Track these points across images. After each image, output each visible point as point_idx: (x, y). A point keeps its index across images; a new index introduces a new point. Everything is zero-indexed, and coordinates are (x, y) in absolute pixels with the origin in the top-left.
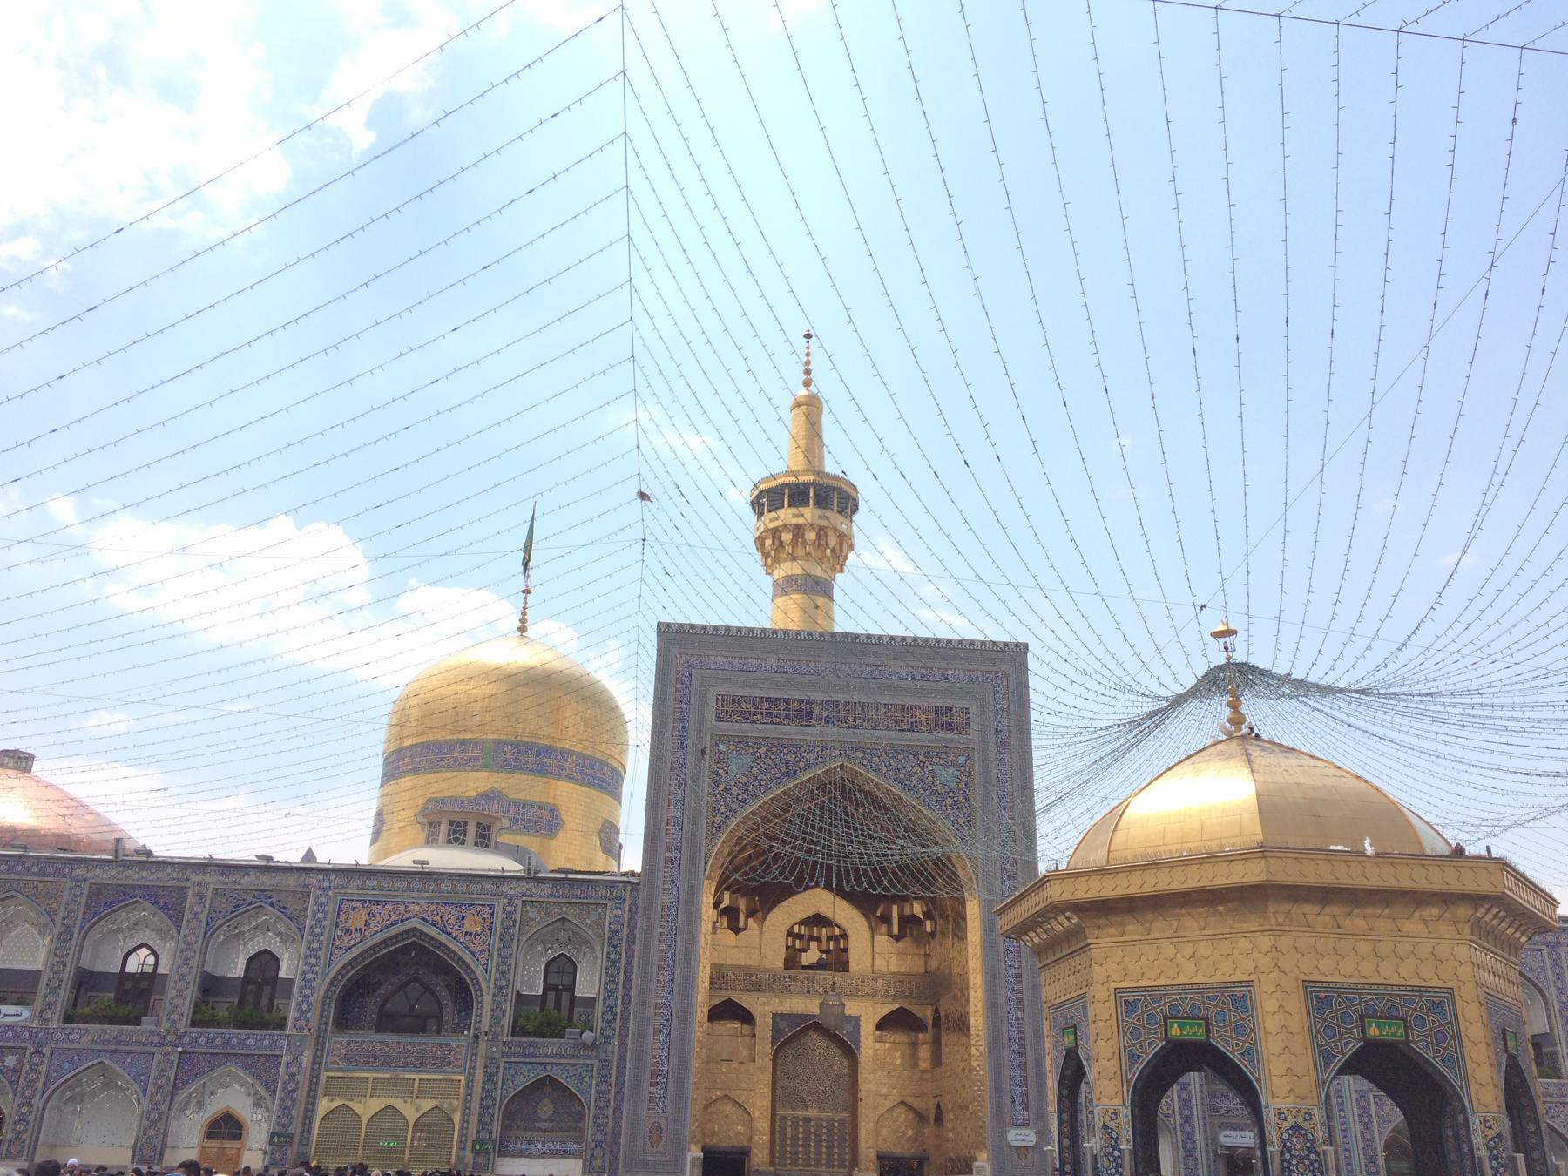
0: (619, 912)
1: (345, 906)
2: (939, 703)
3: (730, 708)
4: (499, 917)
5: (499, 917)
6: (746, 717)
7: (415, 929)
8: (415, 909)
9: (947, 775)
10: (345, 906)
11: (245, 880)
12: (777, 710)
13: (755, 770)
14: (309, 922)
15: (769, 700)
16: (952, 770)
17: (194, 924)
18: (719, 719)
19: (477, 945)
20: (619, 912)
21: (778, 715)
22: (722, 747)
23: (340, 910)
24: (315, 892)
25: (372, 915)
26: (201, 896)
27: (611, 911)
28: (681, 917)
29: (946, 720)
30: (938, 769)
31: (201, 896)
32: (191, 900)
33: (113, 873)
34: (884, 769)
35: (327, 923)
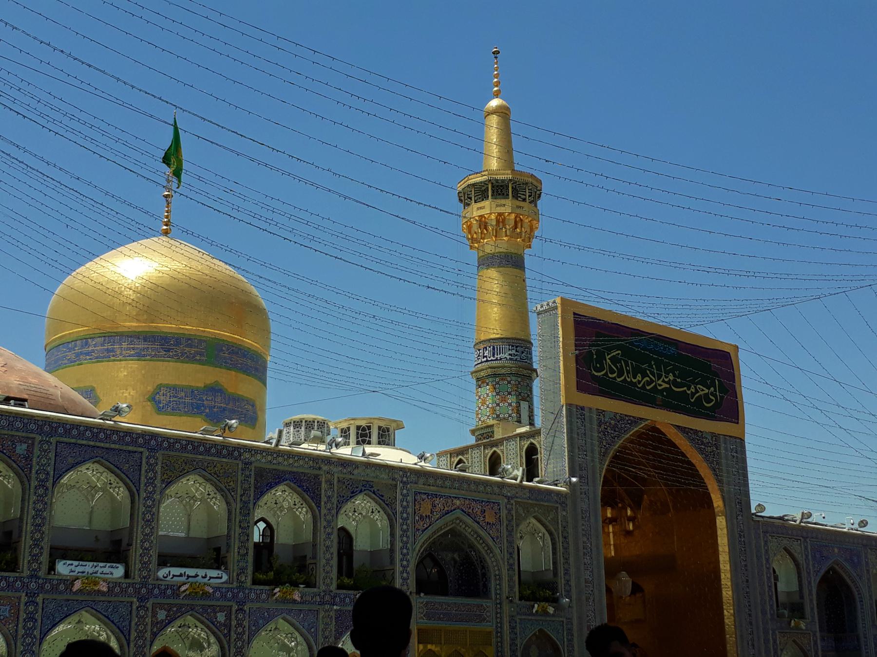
1: (418, 497)
4: (504, 513)
5: (504, 513)
7: (458, 518)
8: (458, 502)
10: (418, 497)
11: (356, 472)
14: (399, 509)
17: (329, 506)
19: (494, 533)
23: (415, 500)
24: (399, 485)
25: (434, 506)
26: (330, 483)
27: (561, 513)
28: (592, 520)
31: (330, 483)
32: (324, 486)
33: (269, 458)
35: (410, 510)
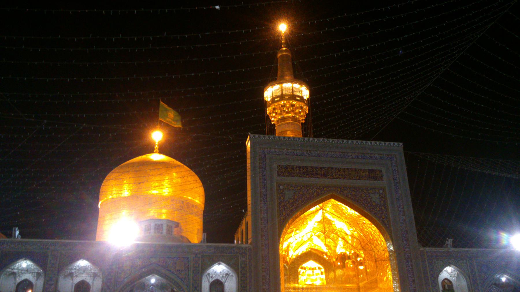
0: (244, 259)
2: (370, 168)
3: (283, 171)
6: (290, 174)
9: (375, 198)
12: (304, 171)
13: (296, 197)
15: (299, 167)
16: (377, 196)
18: (279, 175)
20: (244, 259)
21: (304, 173)
22: (281, 187)
29: (374, 175)
30: (371, 195)
34: (350, 196)
